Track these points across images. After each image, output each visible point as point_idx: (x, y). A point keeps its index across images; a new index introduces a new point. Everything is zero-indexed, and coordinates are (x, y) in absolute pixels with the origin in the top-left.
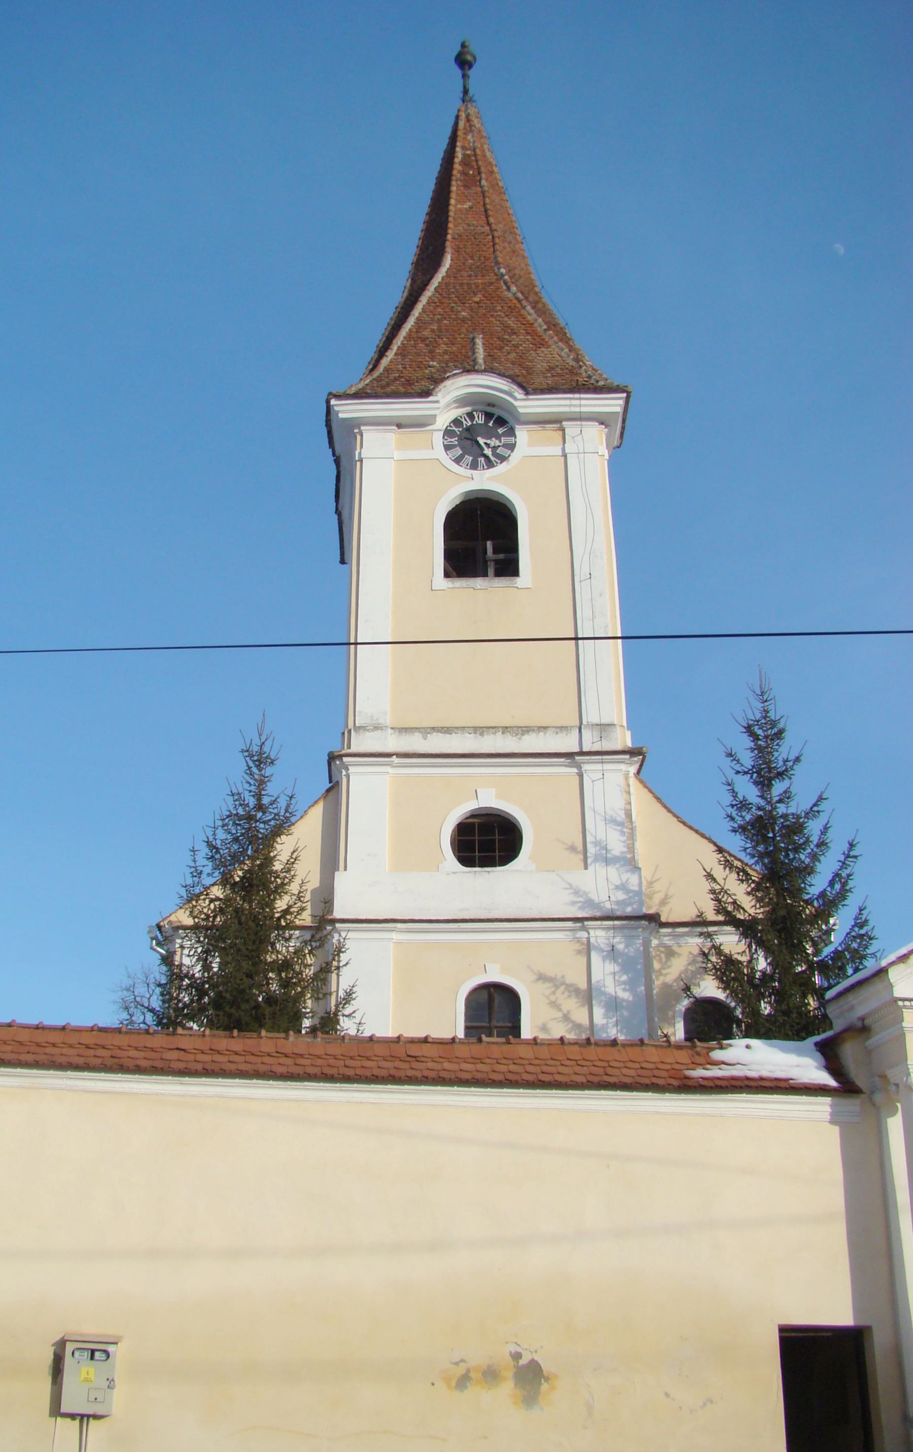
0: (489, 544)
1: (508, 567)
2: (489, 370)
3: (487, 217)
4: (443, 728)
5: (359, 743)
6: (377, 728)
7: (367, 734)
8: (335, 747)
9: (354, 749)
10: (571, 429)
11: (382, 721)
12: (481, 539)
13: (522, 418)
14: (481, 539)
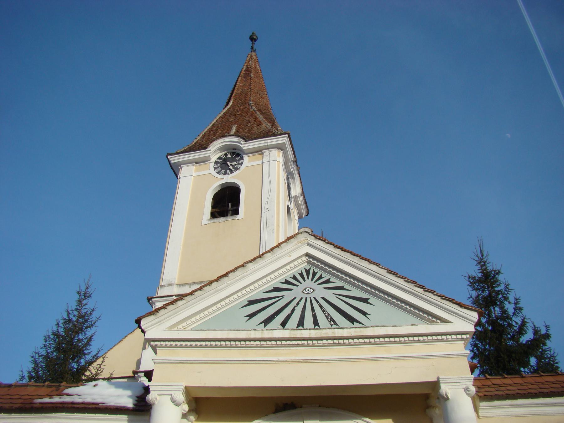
0: (230, 204)
1: (236, 212)
2: (235, 135)
3: (250, 85)
5: (162, 292)
6: (170, 285)
8: (150, 296)
9: (159, 295)
10: (266, 153)
11: (173, 282)
12: (226, 202)
13: (246, 152)
14: (226, 202)
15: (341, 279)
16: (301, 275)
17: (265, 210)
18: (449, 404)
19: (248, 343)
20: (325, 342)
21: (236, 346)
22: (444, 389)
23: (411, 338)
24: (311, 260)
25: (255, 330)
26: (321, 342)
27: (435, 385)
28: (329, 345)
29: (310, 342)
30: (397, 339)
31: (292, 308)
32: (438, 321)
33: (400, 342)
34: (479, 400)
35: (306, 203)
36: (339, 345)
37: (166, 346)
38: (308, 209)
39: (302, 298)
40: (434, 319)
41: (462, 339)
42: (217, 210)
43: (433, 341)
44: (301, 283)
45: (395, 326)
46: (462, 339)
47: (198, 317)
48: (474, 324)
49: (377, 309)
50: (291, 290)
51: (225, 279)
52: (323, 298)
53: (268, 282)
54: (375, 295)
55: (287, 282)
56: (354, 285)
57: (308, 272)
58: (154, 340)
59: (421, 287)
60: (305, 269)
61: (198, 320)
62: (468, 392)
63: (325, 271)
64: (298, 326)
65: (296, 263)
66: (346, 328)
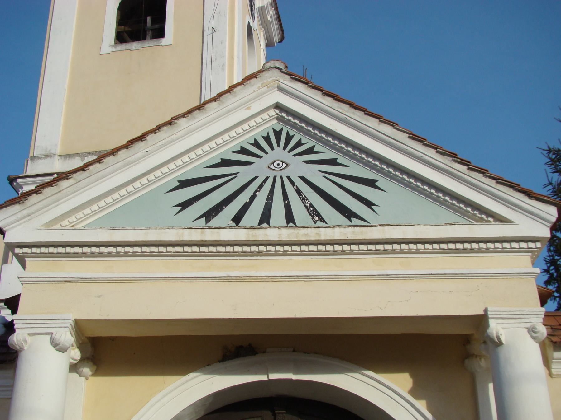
0: (149, 19)
1: (159, 33)
4: (96, 152)
5: (33, 168)
6: (47, 156)
7: (40, 161)
8: (13, 174)
9: (29, 173)
11: (53, 151)
15: (333, 147)
16: (267, 139)
17: (210, 32)
18: (502, 352)
19: (178, 249)
20: (304, 248)
21: (160, 254)
22: (495, 327)
23: (443, 246)
24: (284, 115)
25: (191, 228)
26: (297, 248)
27: (481, 321)
28: (311, 253)
29: (279, 248)
30: (420, 246)
31: (251, 194)
32: (490, 219)
33: (426, 252)
34: (552, 348)
35: (279, 19)
36: (327, 253)
37: (41, 255)
38: (282, 31)
39: (267, 178)
40: (483, 216)
41: (529, 250)
42: (127, 29)
43: (480, 251)
44: (266, 153)
45: (419, 225)
46: (529, 250)
47: (95, 207)
48: (549, 225)
49: (390, 196)
50: (250, 163)
51: (141, 144)
52: (302, 178)
53: (212, 150)
54: (387, 175)
55: (243, 151)
56: (353, 157)
57: (278, 134)
58: (21, 246)
59: (463, 162)
60: (274, 130)
61: (95, 213)
62: (534, 335)
63: (307, 133)
64: (260, 223)
65: (258, 119)
66: (339, 226)
